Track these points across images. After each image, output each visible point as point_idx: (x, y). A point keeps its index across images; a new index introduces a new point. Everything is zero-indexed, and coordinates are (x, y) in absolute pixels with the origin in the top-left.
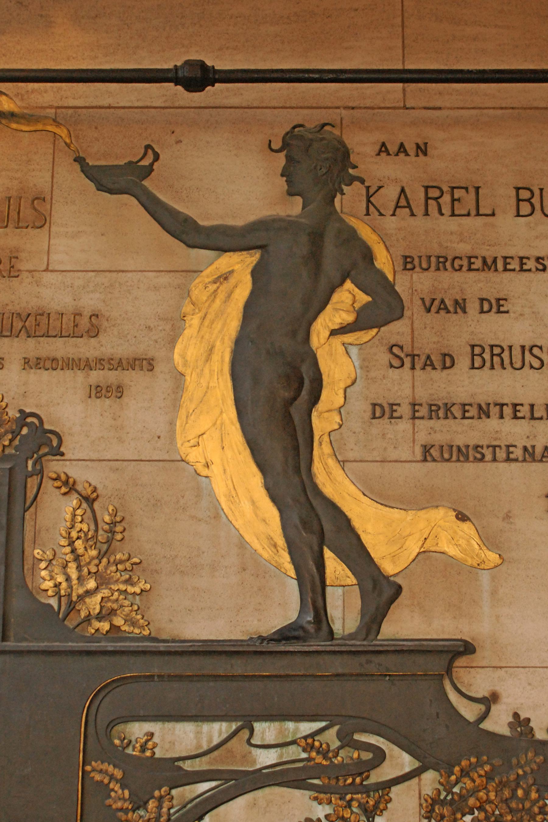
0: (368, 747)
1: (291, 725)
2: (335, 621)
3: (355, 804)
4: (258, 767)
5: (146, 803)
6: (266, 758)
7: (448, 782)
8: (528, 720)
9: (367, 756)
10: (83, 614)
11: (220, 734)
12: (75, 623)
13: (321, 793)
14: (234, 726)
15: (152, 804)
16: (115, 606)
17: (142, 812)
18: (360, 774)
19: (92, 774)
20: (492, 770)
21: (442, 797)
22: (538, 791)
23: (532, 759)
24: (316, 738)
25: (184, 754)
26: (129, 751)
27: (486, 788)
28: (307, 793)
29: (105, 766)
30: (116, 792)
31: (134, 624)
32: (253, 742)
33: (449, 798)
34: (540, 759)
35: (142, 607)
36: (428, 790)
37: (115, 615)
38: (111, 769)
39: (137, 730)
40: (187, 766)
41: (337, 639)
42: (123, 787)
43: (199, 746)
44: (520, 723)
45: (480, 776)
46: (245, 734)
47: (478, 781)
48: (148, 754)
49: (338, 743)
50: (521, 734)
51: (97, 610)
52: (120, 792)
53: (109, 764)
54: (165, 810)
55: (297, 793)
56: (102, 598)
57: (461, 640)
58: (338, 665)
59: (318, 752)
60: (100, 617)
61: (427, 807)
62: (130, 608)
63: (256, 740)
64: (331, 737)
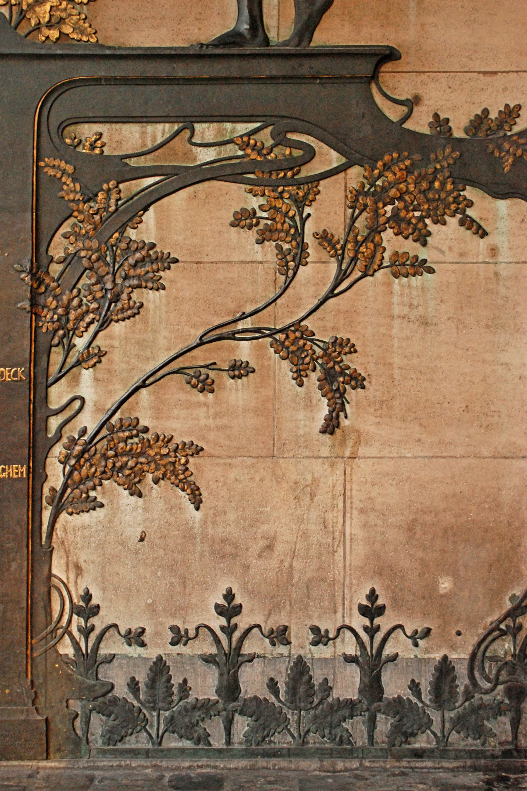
0: (299, 145)
1: (228, 126)
2: (271, 29)
3: (286, 195)
4: (199, 163)
5: (97, 195)
6: (207, 155)
7: (371, 175)
8: (447, 120)
9: (297, 153)
10: (33, 22)
11: (163, 133)
12: (26, 31)
13: (255, 187)
14: (176, 127)
16: (64, 15)
17: (92, 204)
18: (291, 169)
19: (45, 170)
20: (412, 165)
21: (366, 190)
22: (453, 183)
23: (448, 155)
24: (252, 137)
25: (130, 152)
27: (406, 181)
29: (56, 163)
30: (68, 185)
31: (82, 32)
32: (194, 141)
33: (372, 189)
35: (89, 17)
36: (354, 184)
37: (65, 23)
38: (63, 164)
40: (133, 162)
41: (272, 46)
42: (74, 181)
43: (144, 145)
44: (440, 123)
45: (401, 170)
46: (187, 134)
47: (399, 174)
48: (97, 151)
49: (271, 142)
50: (440, 133)
51: (47, 19)
52: (72, 185)
53: (61, 160)
54: (113, 201)
55: (234, 186)
56: (51, 7)
57: (388, 46)
58: (271, 68)
59: (253, 150)
60: (49, 26)
61: (351, 197)
62: (78, 17)
63: (196, 140)
64: (266, 137)
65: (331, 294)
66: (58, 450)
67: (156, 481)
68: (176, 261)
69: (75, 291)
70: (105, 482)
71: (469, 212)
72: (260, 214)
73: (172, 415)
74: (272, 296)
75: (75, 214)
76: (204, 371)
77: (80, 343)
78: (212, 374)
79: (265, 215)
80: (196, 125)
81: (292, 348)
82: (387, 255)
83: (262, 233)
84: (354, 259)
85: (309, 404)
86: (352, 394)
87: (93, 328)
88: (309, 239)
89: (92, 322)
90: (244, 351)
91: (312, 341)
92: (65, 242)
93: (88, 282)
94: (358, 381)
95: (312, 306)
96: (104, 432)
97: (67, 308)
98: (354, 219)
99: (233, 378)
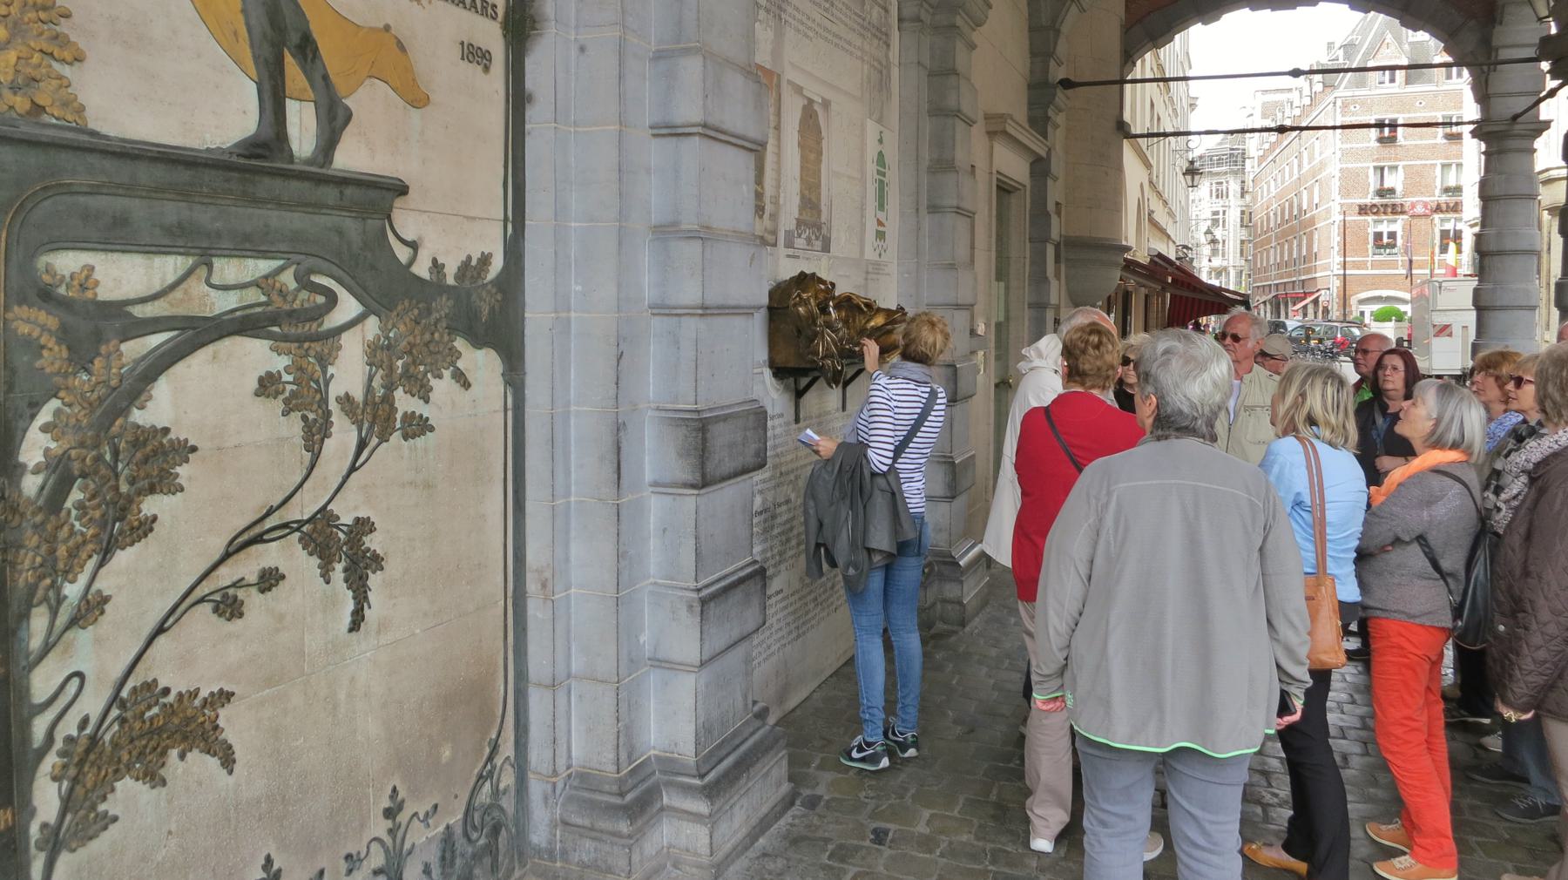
1: (250, 262)
3: (312, 353)
6: (224, 303)
15: (98, 363)
25: (132, 296)
26: (62, 290)
28: (267, 343)
34: (450, 303)
39: (67, 263)
40: (138, 311)
42: (59, 341)
46: (203, 271)
48: (89, 294)
52: (56, 348)
63: (215, 280)
64: (288, 279)
65: (353, 469)
66: (51, 761)
67: (182, 756)
68: (194, 449)
69: (63, 514)
70: (118, 785)
71: (460, 364)
72: (287, 378)
73: (192, 662)
74: (299, 479)
75: (62, 394)
76: (231, 591)
77: (72, 591)
78: (241, 594)
79: (290, 378)
80: (215, 260)
81: (320, 539)
82: (399, 416)
83: (286, 402)
84: (371, 427)
85: (332, 603)
86: (374, 580)
87: (90, 565)
88: (333, 406)
89: (90, 557)
90: (269, 555)
91: (337, 527)
92: (42, 436)
93: (81, 496)
94: (377, 561)
95: (335, 486)
96: (115, 712)
97: (52, 540)
98: (371, 379)
99: (262, 591)
